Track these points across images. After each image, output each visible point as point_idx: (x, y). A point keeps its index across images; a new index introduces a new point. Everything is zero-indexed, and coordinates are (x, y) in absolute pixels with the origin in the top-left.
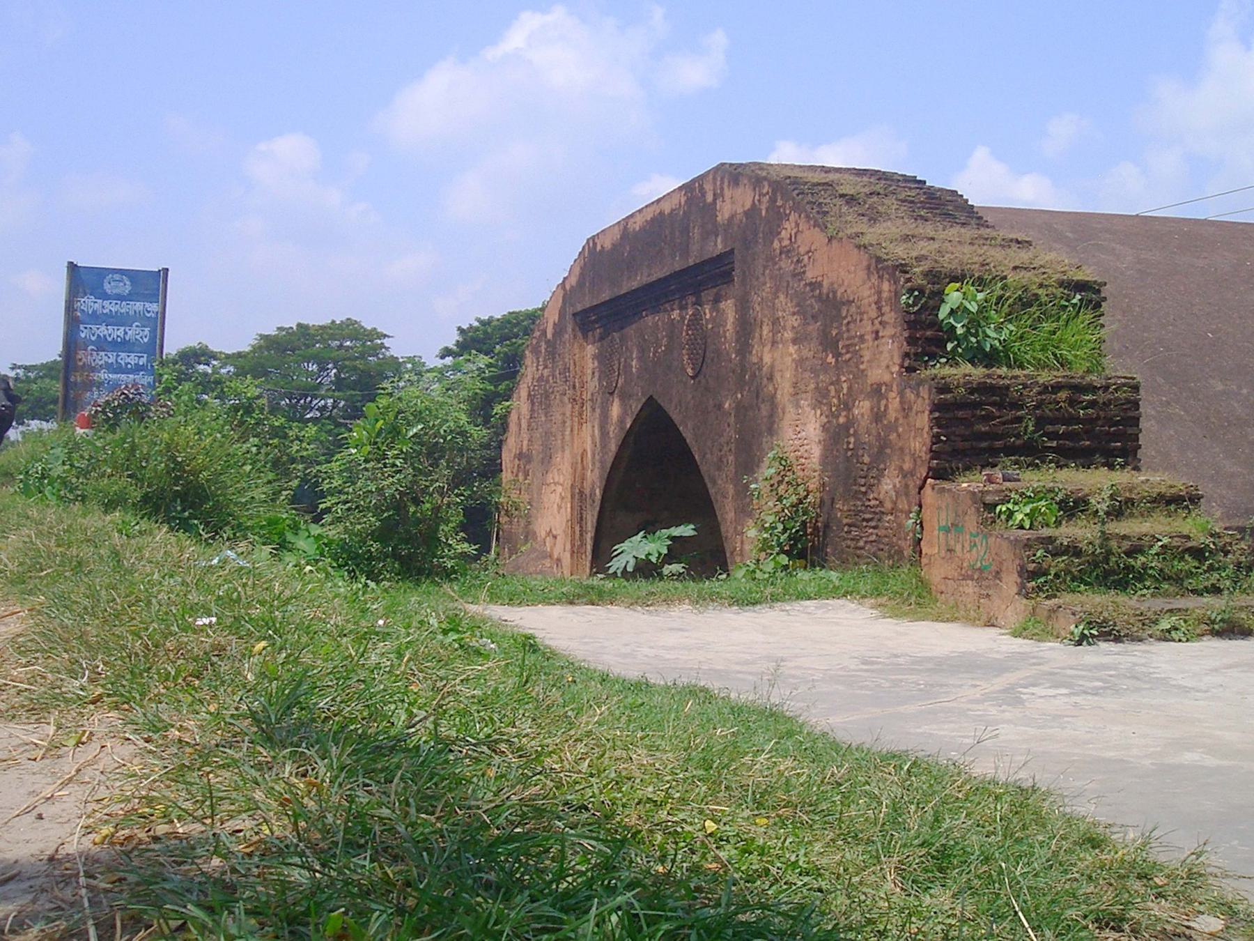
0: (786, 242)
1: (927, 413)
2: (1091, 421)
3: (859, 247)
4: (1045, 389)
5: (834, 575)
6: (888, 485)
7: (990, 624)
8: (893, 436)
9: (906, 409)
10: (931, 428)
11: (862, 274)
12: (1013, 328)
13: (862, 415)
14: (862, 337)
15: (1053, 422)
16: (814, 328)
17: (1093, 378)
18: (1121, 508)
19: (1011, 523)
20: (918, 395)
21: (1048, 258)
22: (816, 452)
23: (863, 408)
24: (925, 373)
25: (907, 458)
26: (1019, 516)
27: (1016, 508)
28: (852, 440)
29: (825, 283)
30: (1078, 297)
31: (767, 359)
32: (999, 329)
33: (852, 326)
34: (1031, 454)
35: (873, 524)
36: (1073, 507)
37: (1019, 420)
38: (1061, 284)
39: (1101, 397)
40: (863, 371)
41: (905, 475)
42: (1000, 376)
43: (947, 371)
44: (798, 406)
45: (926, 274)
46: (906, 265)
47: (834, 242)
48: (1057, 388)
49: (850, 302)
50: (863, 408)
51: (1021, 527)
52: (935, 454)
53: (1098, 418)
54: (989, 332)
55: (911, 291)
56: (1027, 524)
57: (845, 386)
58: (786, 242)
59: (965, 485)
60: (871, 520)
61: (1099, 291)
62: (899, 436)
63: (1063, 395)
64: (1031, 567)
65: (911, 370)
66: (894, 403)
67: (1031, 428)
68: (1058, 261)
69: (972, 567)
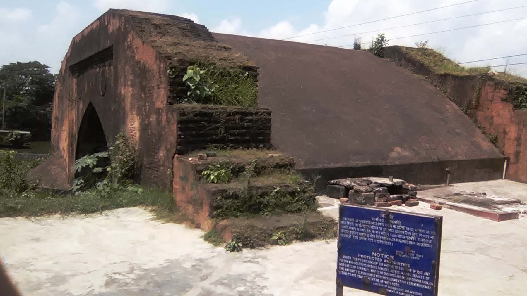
0: (129, 43)
1: (176, 124)
3: (153, 47)
4: (229, 114)
5: (140, 190)
6: (162, 154)
7: (198, 226)
8: (163, 133)
9: (168, 121)
10: (177, 132)
11: (154, 59)
12: (218, 86)
14: (153, 86)
15: (233, 128)
16: (138, 80)
17: (252, 110)
18: (259, 171)
19: (208, 180)
20: (173, 116)
21: (237, 55)
22: (138, 135)
23: (153, 118)
24: (176, 106)
25: (169, 143)
26: (212, 177)
27: (211, 172)
28: (150, 131)
29: (141, 62)
30: (247, 73)
31: (123, 92)
32: (210, 88)
34: (223, 143)
36: (237, 171)
37: (218, 128)
38: (240, 67)
39: (254, 117)
41: (168, 151)
42: (209, 108)
43: (187, 105)
44: (132, 114)
45: (179, 60)
46: (170, 56)
47: (145, 44)
48: (237, 113)
50: (153, 118)
51: (213, 182)
52: (179, 144)
53: (253, 126)
54: (205, 88)
55: (171, 68)
57: (147, 107)
58: (129, 43)
60: (156, 167)
61: (256, 71)
62: (166, 132)
63: (237, 117)
65: (171, 104)
66: (165, 118)
67: (223, 132)
68: (239, 57)
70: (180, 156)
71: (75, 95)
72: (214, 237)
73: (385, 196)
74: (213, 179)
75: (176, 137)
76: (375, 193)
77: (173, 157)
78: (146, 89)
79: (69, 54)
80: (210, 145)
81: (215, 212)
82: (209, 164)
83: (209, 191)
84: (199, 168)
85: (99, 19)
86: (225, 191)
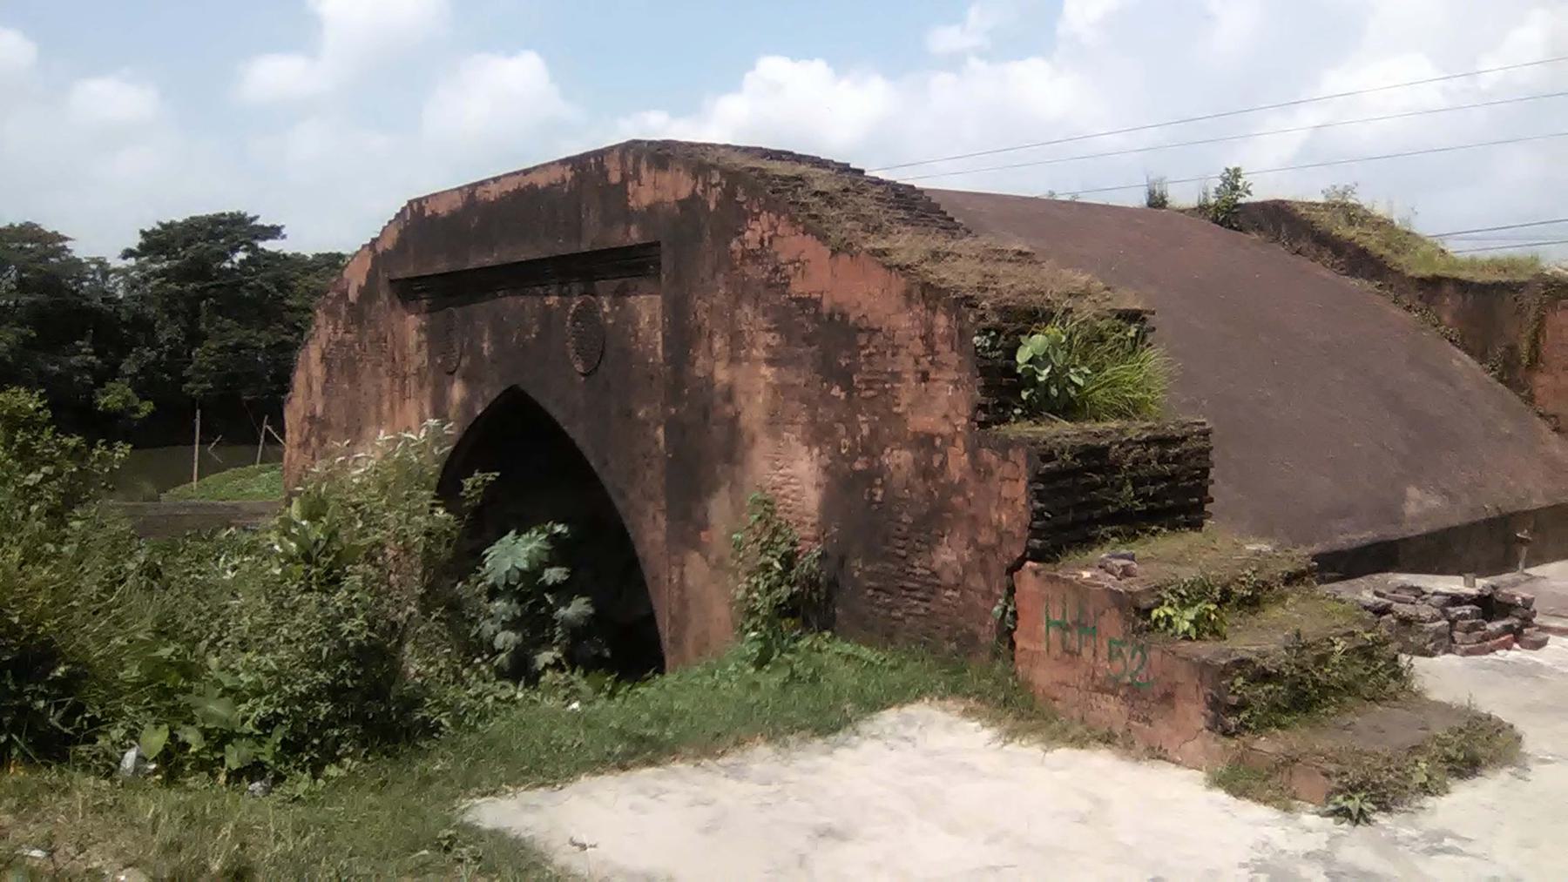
1: (1022, 483)
2: (1173, 477)
6: (949, 555)
7: (1157, 753)
8: (957, 500)
9: (981, 472)
13: (898, 466)
19: (1171, 631)
20: (1006, 459)
22: (812, 499)
29: (826, 303)
31: (722, 375)
33: (877, 358)
35: (920, 595)
40: (898, 415)
48: (1148, 442)
49: (874, 331)
50: (899, 459)
52: (1035, 533)
56: (1193, 634)
58: (754, 245)
59: (1086, 574)
64: (1234, 700)
65: (984, 425)
66: (958, 462)
69: (1116, 680)
70: (1041, 566)
71: (419, 359)
72: (1239, 780)
73: (1474, 627)
74: (1186, 633)
75: (1027, 518)
76: (1453, 622)
77: (1017, 565)
78: (855, 378)
79: (388, 244)
80: (1103, 531)
81: (1232, 721)
82: (1159, 588)
83: (1204, 666)
84: (1145, 603)
85: (578, 163)
86: (1241, 663)
